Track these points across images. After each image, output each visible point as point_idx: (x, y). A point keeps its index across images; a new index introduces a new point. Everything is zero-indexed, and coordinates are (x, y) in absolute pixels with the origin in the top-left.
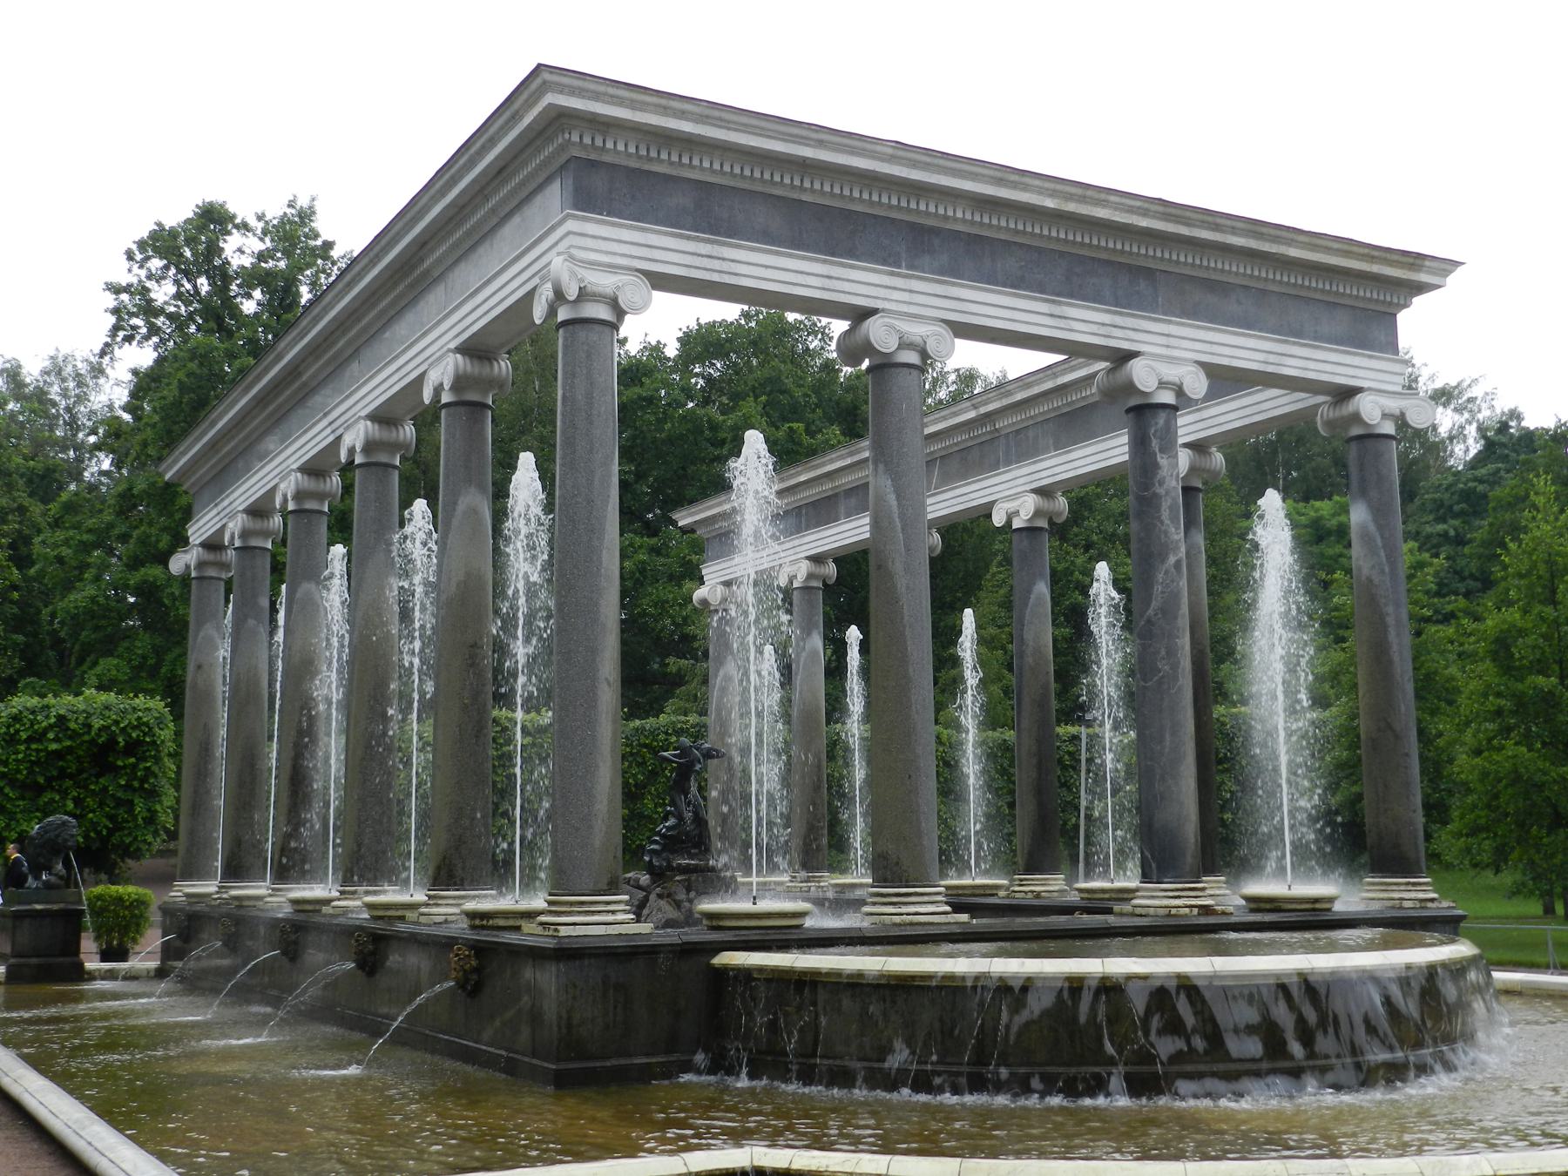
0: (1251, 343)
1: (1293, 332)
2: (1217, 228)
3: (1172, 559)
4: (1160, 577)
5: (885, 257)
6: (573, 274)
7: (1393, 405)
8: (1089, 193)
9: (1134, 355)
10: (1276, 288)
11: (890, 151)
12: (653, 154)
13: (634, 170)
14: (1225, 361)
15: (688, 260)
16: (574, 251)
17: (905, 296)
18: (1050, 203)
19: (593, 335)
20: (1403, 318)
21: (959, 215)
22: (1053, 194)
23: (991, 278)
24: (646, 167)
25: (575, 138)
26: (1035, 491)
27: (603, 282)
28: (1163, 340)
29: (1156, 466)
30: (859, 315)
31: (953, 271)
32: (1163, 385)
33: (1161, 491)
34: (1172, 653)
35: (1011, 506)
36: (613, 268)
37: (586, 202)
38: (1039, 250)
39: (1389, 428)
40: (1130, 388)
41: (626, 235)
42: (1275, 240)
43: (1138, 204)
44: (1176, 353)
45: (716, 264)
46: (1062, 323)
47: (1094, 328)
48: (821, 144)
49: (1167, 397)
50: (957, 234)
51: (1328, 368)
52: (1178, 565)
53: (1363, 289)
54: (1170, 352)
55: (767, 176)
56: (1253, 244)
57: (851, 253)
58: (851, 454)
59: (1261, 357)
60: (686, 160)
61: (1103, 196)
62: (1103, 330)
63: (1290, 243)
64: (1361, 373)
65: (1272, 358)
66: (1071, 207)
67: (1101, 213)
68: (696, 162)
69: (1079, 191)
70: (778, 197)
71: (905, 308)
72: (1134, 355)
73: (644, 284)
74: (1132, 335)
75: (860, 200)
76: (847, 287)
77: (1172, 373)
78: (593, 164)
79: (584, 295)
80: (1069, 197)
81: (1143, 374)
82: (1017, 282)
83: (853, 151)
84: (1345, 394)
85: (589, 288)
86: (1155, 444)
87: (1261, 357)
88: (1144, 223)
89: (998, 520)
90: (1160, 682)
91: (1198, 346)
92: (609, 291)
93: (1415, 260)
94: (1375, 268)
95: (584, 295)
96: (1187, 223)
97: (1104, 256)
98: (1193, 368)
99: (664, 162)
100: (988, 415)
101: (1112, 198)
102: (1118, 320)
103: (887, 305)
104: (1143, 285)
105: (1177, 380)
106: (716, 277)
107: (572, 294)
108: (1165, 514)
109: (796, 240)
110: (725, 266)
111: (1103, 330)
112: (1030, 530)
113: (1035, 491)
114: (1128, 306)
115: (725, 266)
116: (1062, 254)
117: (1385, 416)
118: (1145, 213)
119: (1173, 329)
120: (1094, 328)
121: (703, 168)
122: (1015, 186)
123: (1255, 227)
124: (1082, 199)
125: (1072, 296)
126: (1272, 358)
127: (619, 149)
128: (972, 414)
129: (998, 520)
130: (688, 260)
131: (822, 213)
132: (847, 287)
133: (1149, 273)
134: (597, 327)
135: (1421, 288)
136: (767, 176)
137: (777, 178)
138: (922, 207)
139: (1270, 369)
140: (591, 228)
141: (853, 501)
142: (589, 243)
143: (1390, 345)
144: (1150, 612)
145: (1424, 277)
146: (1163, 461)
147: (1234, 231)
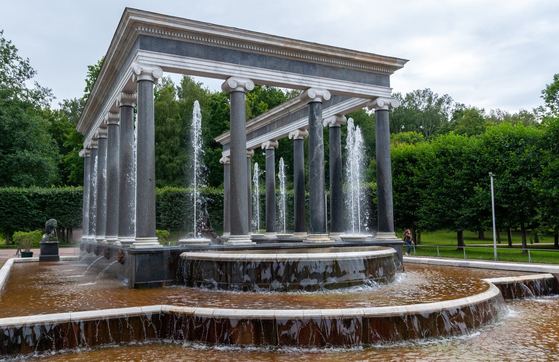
0: (345, 84)
1: (359, 81)
2: (333, 51)
3: (319, 145)
4: (316, 150)
5: (233, 61)
6: (139, 67)
7: (388, 101)
9: (309, 88)
10: (352, 69)
11: (232, 30)
12: (163, 33)
13: (158, 38)
14: (337, 89)
15: (174, 63)
16: (140, 61)
17: (240, 72)
18: (282, 45)
19: (147, 84)
20: (391, 76)
21: (255, 49)
22: (282, 42)
23: (265, 67)
24: (162, 37)
25: (139, 29)
26: (299, 129)
27: (148, 69)
28: (318, 84)
29: (315, 119)
30: (227, 77)
31: (254, 65)
32: (317, 96)
33: (317, 126)
34: (318, 171)
35: (293, 133)
36: (151, 65)
37: (144, 47)
38: (280, 59)
39: (386, 108)
40: (308, 97)
41: (155, 56)
42: (351, 54)
44: (321, 87)
45: (183, 64)
46: (287, 79)
47: (297, 80)
48: (213, 29)
49: (319, 100)
50: (255, 55)
51: (368, 91)
52: (321, 146)
53: (379, 69)
54: (320, 87)
55: (191, 38)
56: (344, 56)
57: (223, 60)
58: (255, 121)
59: (348, 88)
60: (173, 35)
61: (298, 42)
62: (299, 81)
63: (355, 55)
64: (378, 92)
65: (351, 88)
66: (288, 46)
68: (176, 35)
69: (291, 41)
70: (201, 45)
71: (239, 76)
72: (309, 88)
73: (160, 70)
75: (224, 44)
76: (221, 70)
77: (319, 93)
78: (145, 36)
79: (142, 73)
80: (288, 43)
81: (311, 93)
82: (273, 68)
83: (221, 31)
84: (374, 98)
85: (144, 71)
86: (315, 113)
87: (348, 88)
88: (311, 50)
89: (290, 138)
90: (315, 179)
91: (328, 85)
92: (150, 72)
93: (395, 60)
94: (382, 62)
95: (142, 73)
96: (324, 50)
97: (300, 60)
98: (326, 91)
99: (167, 35)
100: (287, 108)
101: (301, 43)
102: (304, 78)
103: (234, 75)
104: (312, 68)
106: (182, 68)
107: (139, 72)
108: (317, 133)
109: (206, 57)
110: (185, 64)
111: (299, 81)
112: (298, 140)
113: (299, 129)
114: (307, 74)
115: (185, 64)
116: (287, 60)
117: (385, 104)
118: (312, 47)
119: (320, 80)
120: (297, 80)
121: (177, 37)
122: (271, 40)
123: (345, 51)
124: (292, 44)
125: (290, 72)
126: (351, 88)
127: (154, 32)
128: (283, 108)
129: (290, 138)
130: (174, 63)
131: (214, 49)
132: (221, 70)
133: (314, 65)
134: (147, 82)
135: (396, 68)
136: (197, 39)
137: (200, 39)
138: (244, 47)
139: (350, 91)
140: (144, 54)
141: (256, 134)
142: (144, 58)
143: (388, 85)
144: (313, 160)
145: (397, 65)
146: (317, 118)
147: (338, 52)
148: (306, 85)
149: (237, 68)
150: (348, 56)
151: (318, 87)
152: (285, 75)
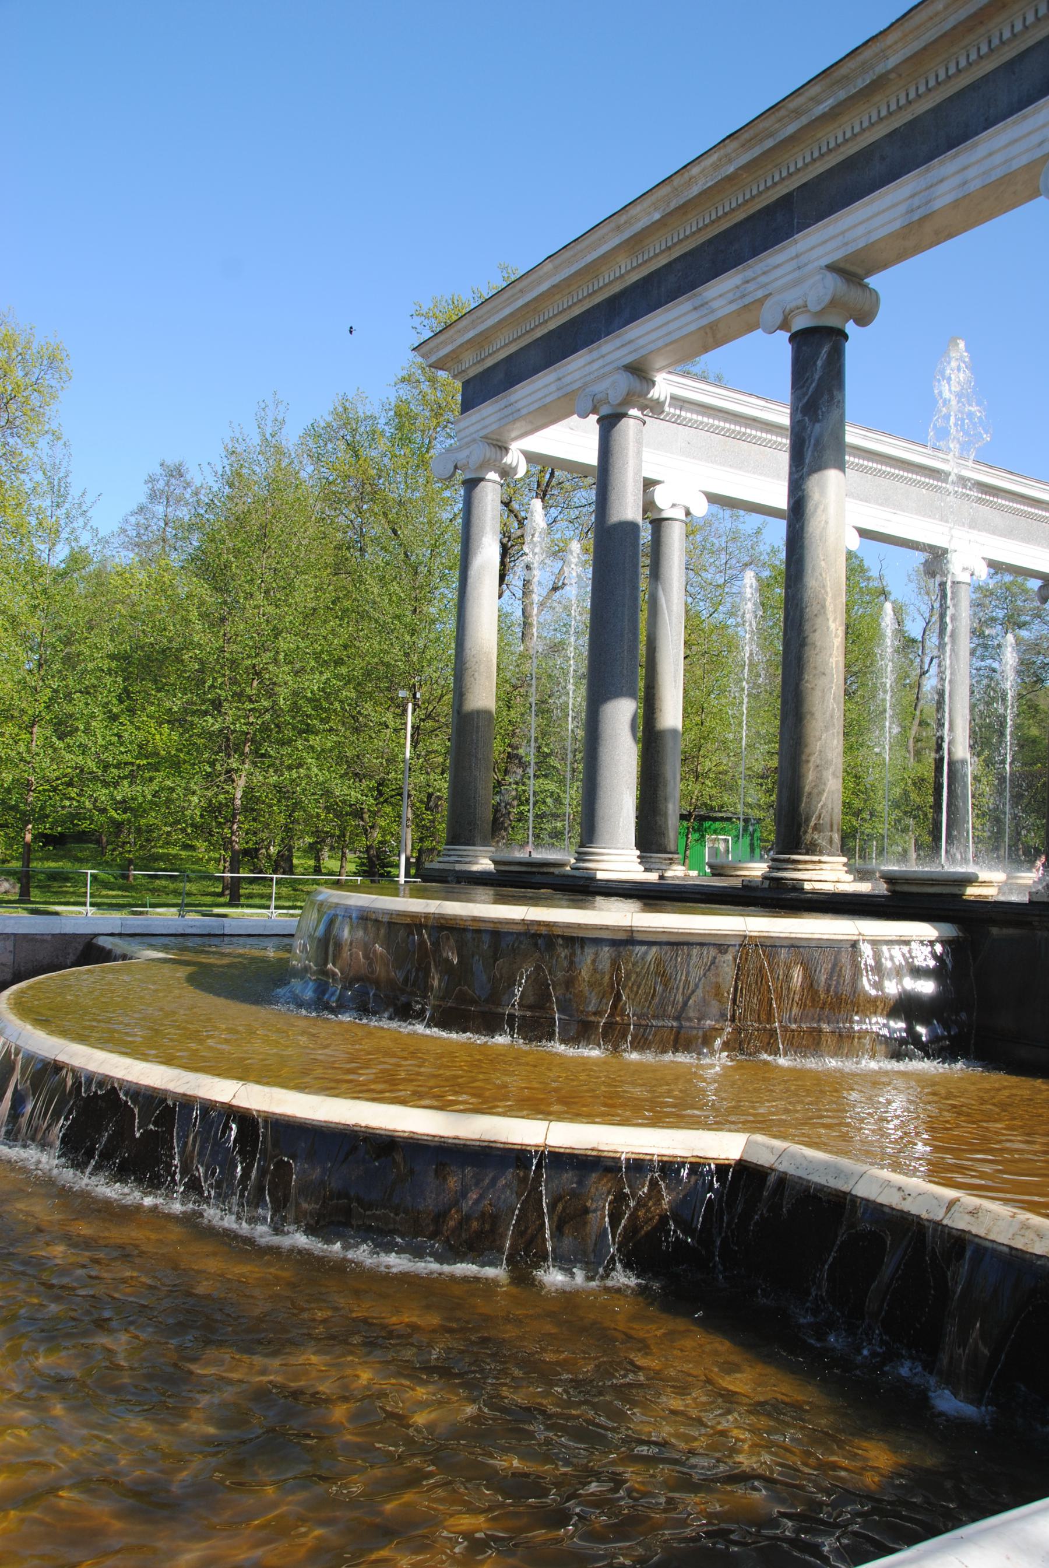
8: (676, 181)
17: (600, 363)
18: (657, 216)
28: (794, 264)
43: (715, 157)
45: (509, 410)
47: (730, 296)
50: (636, 285)
51: (998, 159)
56: (842, 95)
66: (673, 205)
67: (695, 190)
74: (763, 279)
101: (695, 170)
102: (749, 274)
105: (800, 302)
126: (916, 201)
132: (568, 380)
133: (786, 201)
148: (759, 294)
149: (595, 354)
150: (860, 84)
151: (796, 274)
152: (697, 301)
